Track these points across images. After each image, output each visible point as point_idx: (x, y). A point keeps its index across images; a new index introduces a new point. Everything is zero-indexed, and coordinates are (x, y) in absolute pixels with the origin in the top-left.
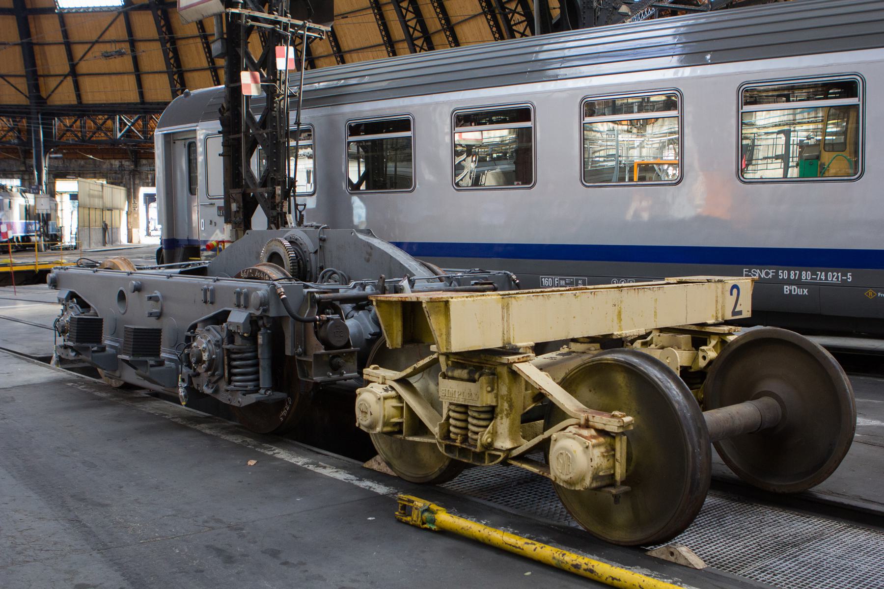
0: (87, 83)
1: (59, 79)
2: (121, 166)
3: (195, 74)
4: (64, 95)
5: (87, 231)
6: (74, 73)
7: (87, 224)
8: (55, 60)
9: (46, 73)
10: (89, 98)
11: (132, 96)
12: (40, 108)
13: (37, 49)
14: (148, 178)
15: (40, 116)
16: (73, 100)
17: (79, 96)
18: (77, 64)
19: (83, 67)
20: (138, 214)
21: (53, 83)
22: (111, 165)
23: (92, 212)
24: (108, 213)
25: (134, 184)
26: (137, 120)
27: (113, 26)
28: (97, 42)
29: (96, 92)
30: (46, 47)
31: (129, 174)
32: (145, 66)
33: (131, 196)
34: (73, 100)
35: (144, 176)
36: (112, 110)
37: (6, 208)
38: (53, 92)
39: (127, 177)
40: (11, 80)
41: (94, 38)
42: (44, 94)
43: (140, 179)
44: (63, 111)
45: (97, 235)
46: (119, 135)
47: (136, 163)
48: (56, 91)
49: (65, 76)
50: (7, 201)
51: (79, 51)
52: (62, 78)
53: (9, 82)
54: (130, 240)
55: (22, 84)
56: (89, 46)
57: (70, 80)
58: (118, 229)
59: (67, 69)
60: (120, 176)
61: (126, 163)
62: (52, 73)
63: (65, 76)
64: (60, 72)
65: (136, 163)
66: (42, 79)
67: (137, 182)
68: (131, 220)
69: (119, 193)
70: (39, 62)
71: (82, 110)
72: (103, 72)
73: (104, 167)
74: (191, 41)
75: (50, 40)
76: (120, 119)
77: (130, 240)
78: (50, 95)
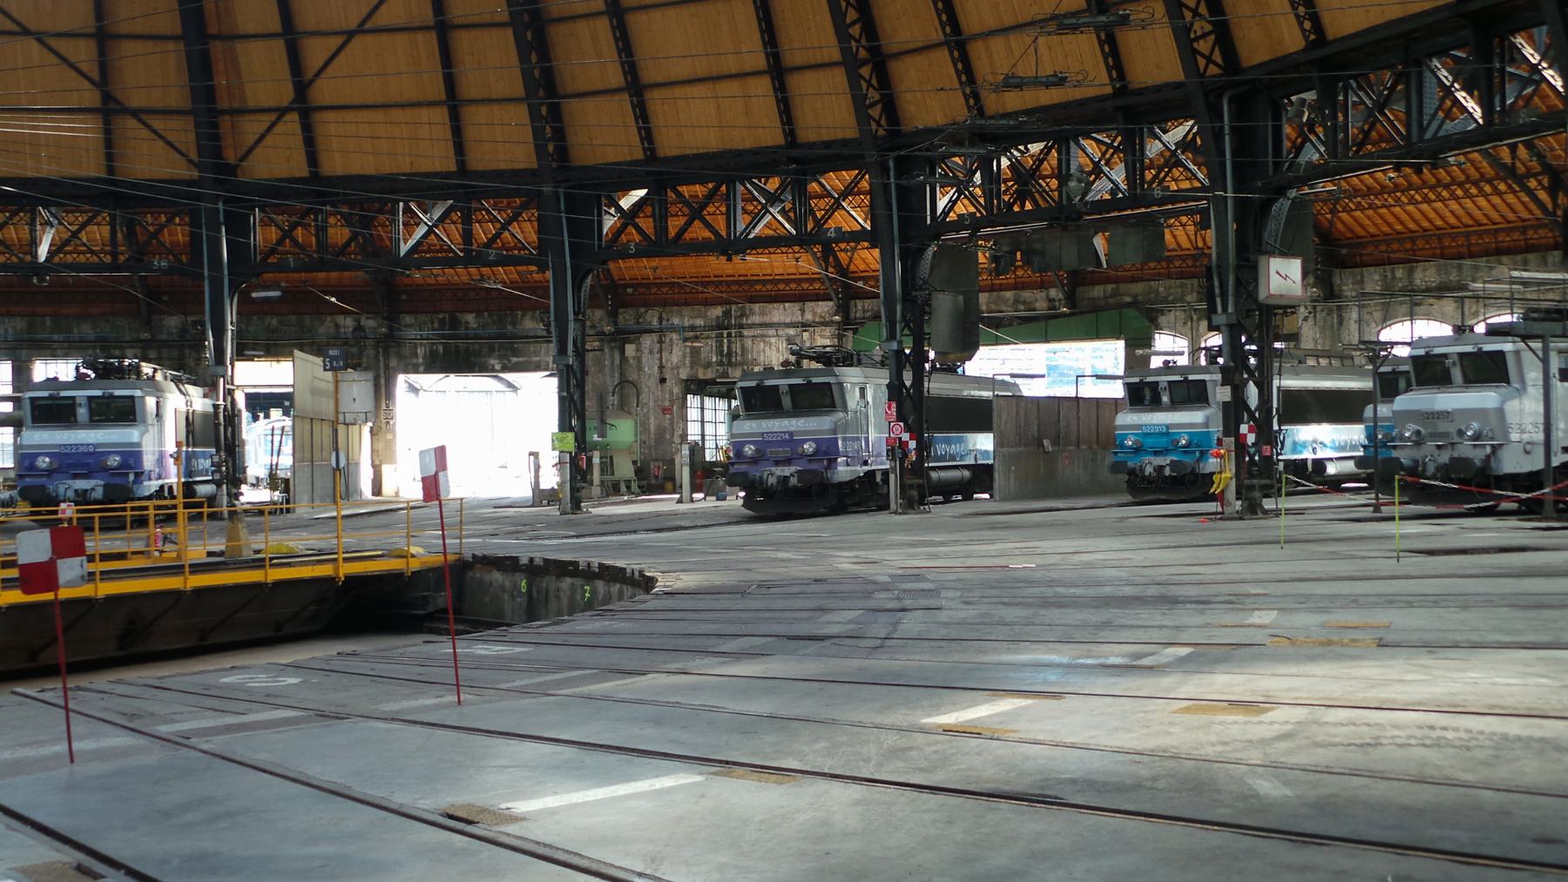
0: (330, 127)
1: (268, 119)
2: (359, 328)
3: (589, 102)
4: (278, 158)
5: (308, 471)
6: (303, 106)
7: (307, 455)
8: (260, 74)
9: (236, 105)
10: (336, 163)
11: (437, 157)
12: (222, 187)
13: (217, 48)
14: (416, 355)
15: (220, 206)
16: (300, 169)
17: (313, 159)
18: (312, 81)
19: (323, 92)
20: (393, 432)
21: (252, 127)
22: (337, 326)
23: (317, 427)
25: (387, 367)
26: (442, 219)
28: (361, 30)
29: (352, 150)
30: (240, 46)
31: (376, 347)
32: (470, 86)
33: (383, 392)
34: (300, 169)
35: (407, 351)
36: (377, 196)
37: (151, 418)
38: (251, 149)
39: (371, 352)
40: (158, 123)
41: (353, 24)
42: (231, 157)
43: (400, 357)
44: (276, 193)
45: (324, 482)
46: (404, 249)
47: (392, 318)
48: (258, 150)
49: (282, 112)
50: (151, 402)
51: (315, 52)
52: (274, 117)
53: (147, 126)
54: (377, 489)
55: (183, 132)
56: (338, 40)
57: (292, 123)
58: (357, 464)
59: (286, 94)
60: (354, 350)
61: (369, 323)
62: (251, 104)
63: (282, 112)
64: (273, 104)
65: (392, 318)
66: (227, 118)
67: (393, 362)
68: (380, 446)
69: (357, 388)
70: (221, 81)
71: (316, 190)
72: (370, 101)
73: (322, 330)
74: (582, 27)
75: (250, 28)
76: (408, 210)
77: (377, 489)
78: (244, 157)
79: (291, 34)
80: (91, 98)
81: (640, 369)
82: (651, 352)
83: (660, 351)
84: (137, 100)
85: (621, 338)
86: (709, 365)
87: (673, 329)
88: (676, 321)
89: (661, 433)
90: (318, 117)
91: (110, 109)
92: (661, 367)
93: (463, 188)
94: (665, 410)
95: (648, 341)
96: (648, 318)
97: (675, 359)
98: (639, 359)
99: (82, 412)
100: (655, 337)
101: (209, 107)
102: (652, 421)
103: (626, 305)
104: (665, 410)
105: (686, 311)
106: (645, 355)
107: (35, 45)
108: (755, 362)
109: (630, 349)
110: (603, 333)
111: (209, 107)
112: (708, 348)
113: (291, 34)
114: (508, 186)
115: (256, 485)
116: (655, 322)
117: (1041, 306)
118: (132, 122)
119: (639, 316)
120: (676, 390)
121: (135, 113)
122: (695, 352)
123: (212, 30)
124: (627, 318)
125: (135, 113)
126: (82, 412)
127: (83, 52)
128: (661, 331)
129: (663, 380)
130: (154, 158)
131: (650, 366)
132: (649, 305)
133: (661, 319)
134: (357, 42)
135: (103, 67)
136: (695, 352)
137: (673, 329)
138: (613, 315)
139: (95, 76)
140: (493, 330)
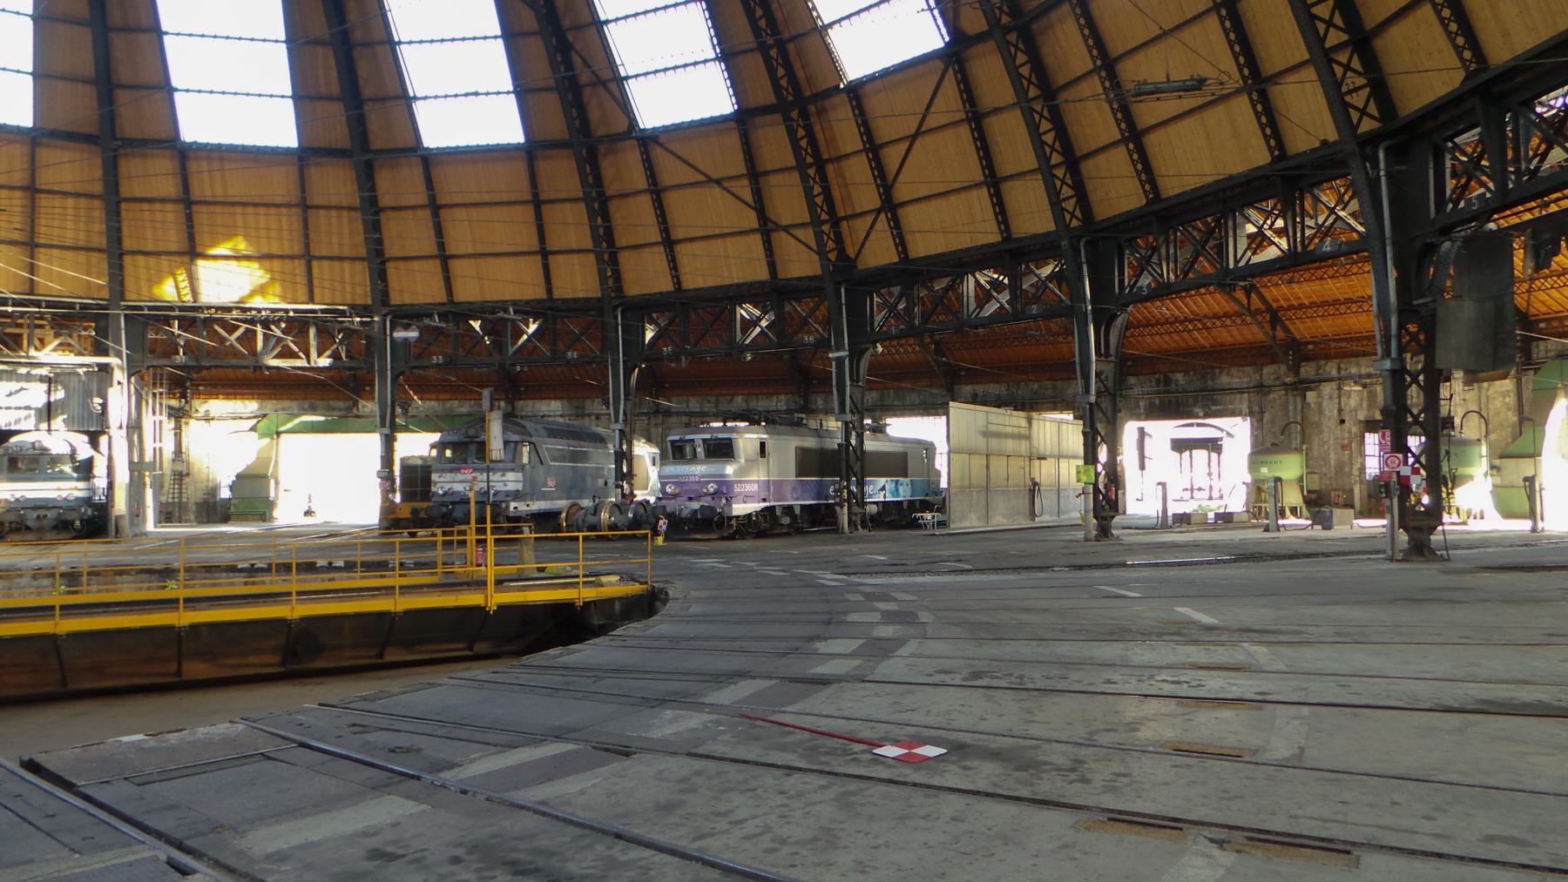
0: (912, 217)
6: (890, 206)
8: (858, 186)
9: (849, 212)
10: (921, 247)
11: (989, 234)
19: (902, 192)
21: (862, 225)
24: (1037, 462)
27: (940, 93)
30: (845, 164)
38: (863, 245)
40: (799, 233)
42: (851, 252)
44: (882, 277)
49: (878, 211)
51: (892, 157)
56: (905, 145)
71: (910, 272)
79: (873, 149)
80: (750, 220)
81: (1321, 412)
82: (1331, 398)
83: (1339, 397)
84: (785, 222)
85: (1301, 387)
87: (1350, 377)
88: (1354, 370)
89: (1340, 466)
90: (901, 212)
91: (767, 228)
92: (1340, 410)
93: (1011, 254)
94: (1344, 447)
95: (1328, 389)
96: (1328, 368)
97: (1353, 402)
98: (1320, 405)
100: (1334, 385)
101: (828, 216)
102: (1332, 455)
103: (1308, 359)
104: (1344, 447)
105: (1363, 361)
106: (1324, 399)
107: (717, 190)
109: (1311, 396)
110: (1285, 384)
111: (828, 216)
113: (873, 149)
114: (1041, 248)
116: (1334, 373)
118: (783, 234)
119: (1319, 368)
120: (1354, 429)
121: (786, 229)
123: (826, 156)
124: (1308, 370)
125: (786, 229)
128: (1341, 379)
129: (1343, 421)
130: (800, 262)
131: (1331, 410)
132: (1328, 357)
133: (1339, 369)
137: (1350, 377)
138: (1295, 369)
140: (1197, 385)
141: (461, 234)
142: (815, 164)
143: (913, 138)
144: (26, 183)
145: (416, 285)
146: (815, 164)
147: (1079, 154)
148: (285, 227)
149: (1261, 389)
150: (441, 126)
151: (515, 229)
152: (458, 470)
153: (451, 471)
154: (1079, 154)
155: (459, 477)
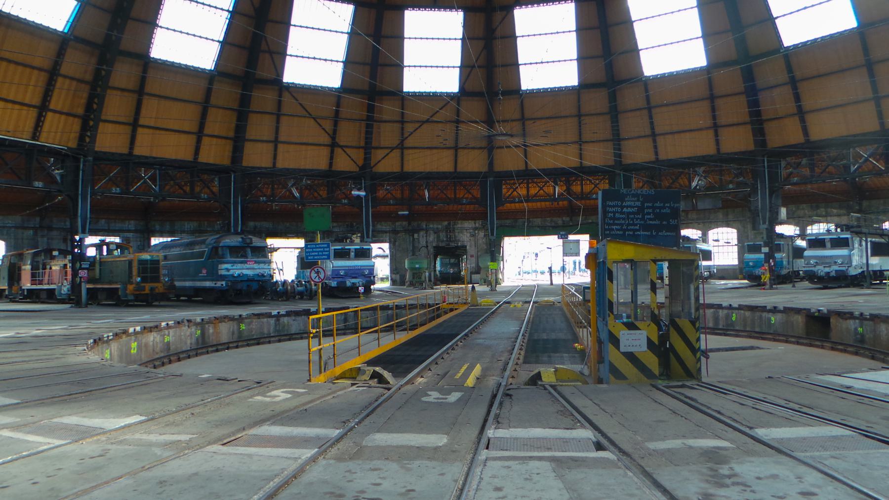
1: (387, 151)
19: (409, 142)
21: (380, 153)
30: (383, 125)
40: (348, 150)
42: (373, 163)
49: (392, 149)
62: (383, 144)
63: (392, 149)
84: (342, 144)
86: (443, 241)
91: (333, 145)
95: (422, 233)
98: (418, 239)
99: (352, 254)
101: (368, 147)
106: (422, 239)
107: (312, 120)
108: (459, 241)
109: (416, 236)
112: (443, 236)
115: (382, 279)
117: (560, 222)
121: (342, 147)
122: (438, 237)
125: (342, 147)
126: (352, 254)
127: (328, 125)
128: (427, 231)
131: (423, 242)
134: (425, 126)
135: (335, 131)
136: (438, 237)
139: (331, 133)
141: (151, 112)
142: (370, 121)
143: (423, 122)
144: (577, 139)
145: (110, 140)
146: (370, 121)
147: (111, 84)
148: (32, 83)
149: (395, 232)
150: (296, 72)
151: (186, 117)
152: (246, 262)
153: (241, 262)
154: (111, 84)
155: (247, 266)
